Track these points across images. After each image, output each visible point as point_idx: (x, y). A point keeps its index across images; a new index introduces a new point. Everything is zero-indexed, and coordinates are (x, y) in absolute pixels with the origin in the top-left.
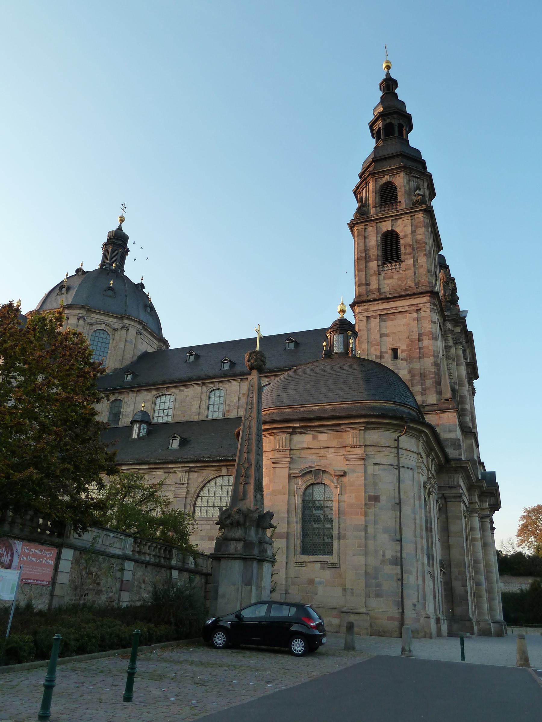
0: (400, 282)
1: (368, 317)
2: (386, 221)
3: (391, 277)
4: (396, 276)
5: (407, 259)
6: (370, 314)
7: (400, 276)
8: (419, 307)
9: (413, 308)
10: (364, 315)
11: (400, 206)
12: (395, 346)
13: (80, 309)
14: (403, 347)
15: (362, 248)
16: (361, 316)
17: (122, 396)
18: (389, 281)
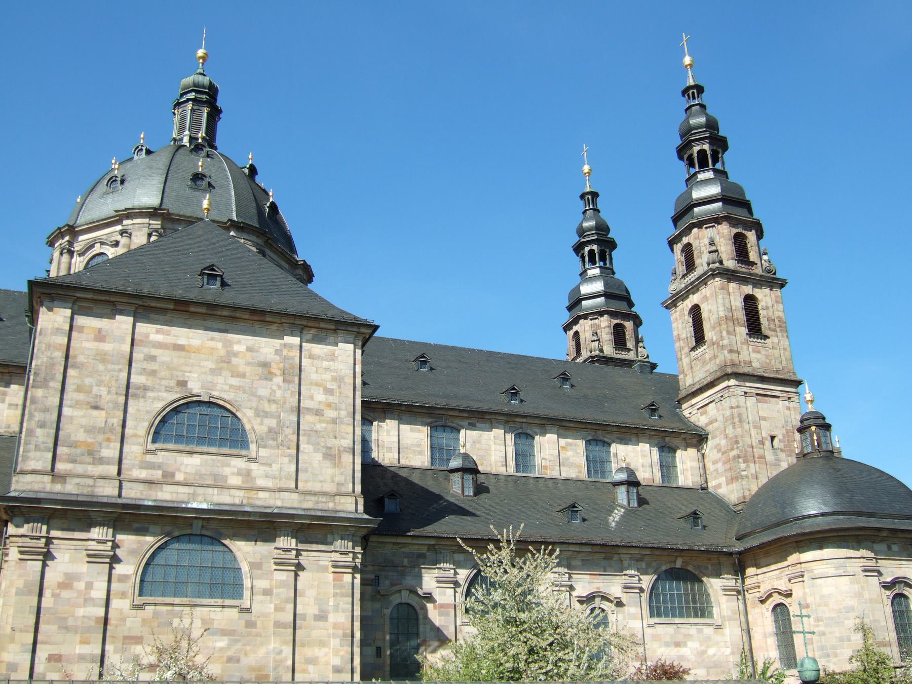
0: (768, 361)
1: (746, 393)
2: (748, 282)
3: (759, 352)
4: (763, 351)
5: (772, 336)
6: (748, 390)
7: (767, 354)
8: (790, 395)
9: (785, 395)
10: (742, 390)
11: (756, 268)
12: (773, 434)
13: (258, 237)
14: (780, 437)
15: (728, 305)
16: (739, 389)
17: (371, 414)
18: (759, 356)
